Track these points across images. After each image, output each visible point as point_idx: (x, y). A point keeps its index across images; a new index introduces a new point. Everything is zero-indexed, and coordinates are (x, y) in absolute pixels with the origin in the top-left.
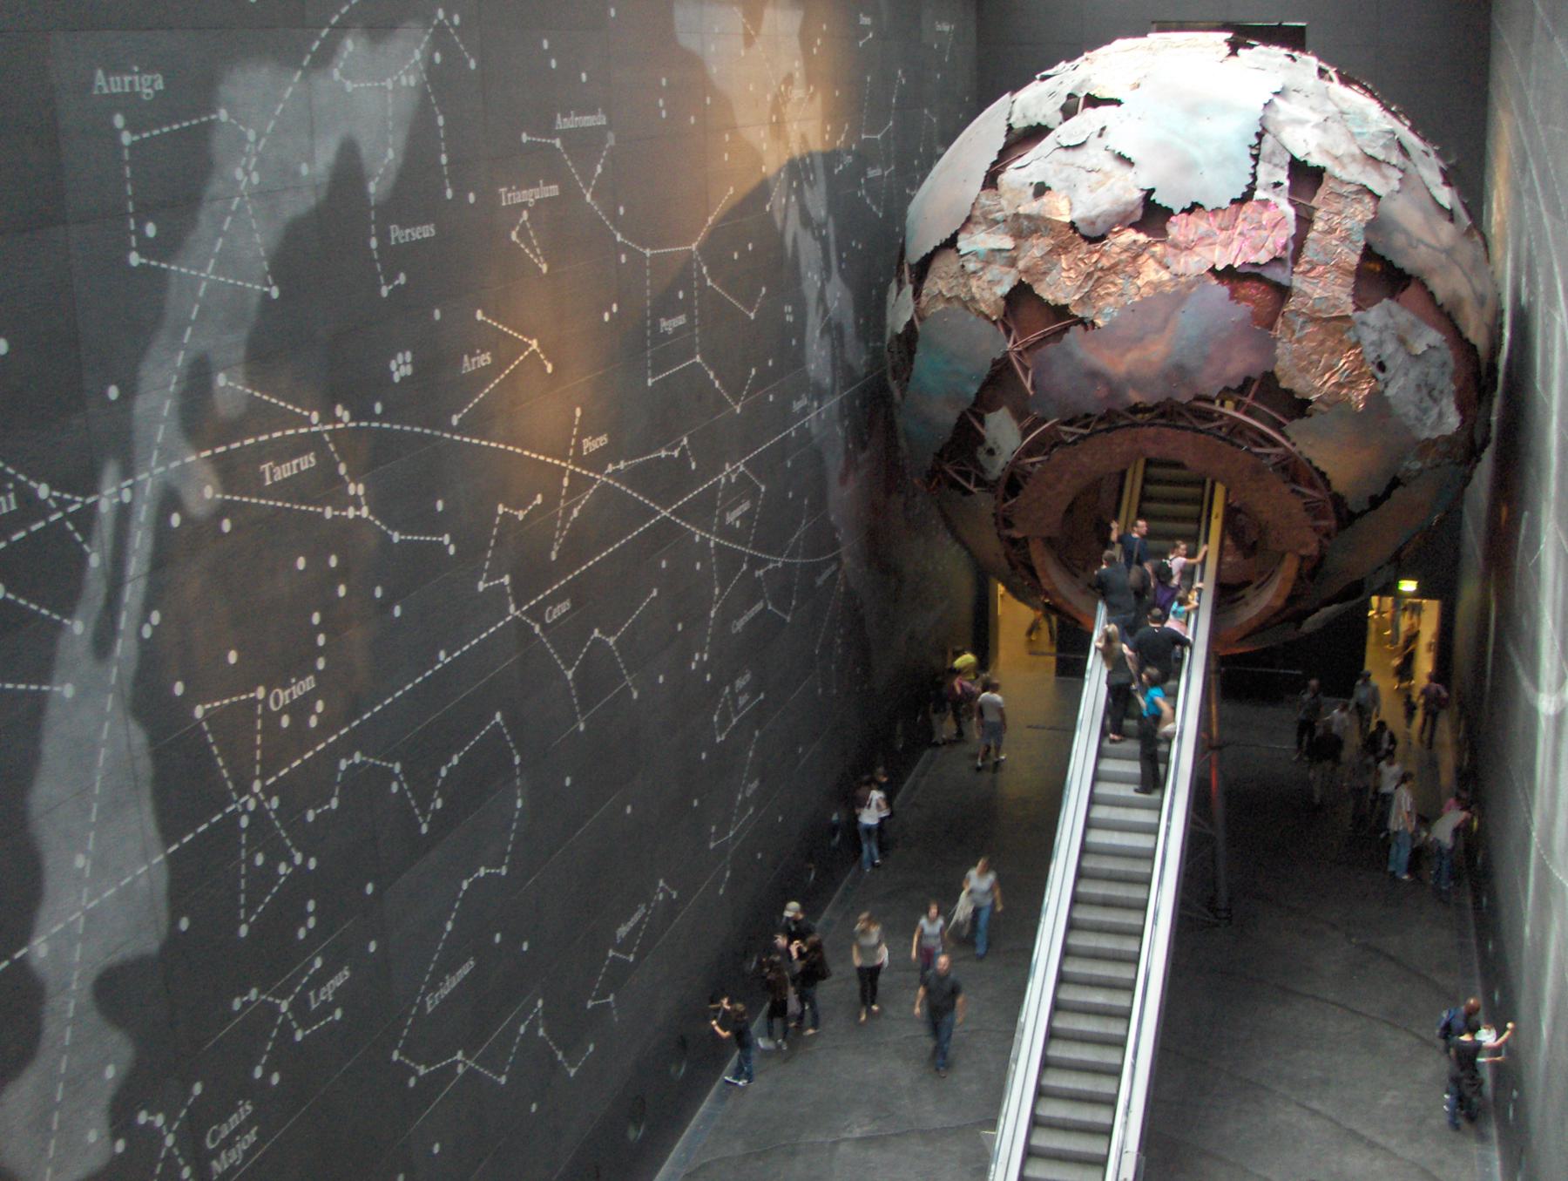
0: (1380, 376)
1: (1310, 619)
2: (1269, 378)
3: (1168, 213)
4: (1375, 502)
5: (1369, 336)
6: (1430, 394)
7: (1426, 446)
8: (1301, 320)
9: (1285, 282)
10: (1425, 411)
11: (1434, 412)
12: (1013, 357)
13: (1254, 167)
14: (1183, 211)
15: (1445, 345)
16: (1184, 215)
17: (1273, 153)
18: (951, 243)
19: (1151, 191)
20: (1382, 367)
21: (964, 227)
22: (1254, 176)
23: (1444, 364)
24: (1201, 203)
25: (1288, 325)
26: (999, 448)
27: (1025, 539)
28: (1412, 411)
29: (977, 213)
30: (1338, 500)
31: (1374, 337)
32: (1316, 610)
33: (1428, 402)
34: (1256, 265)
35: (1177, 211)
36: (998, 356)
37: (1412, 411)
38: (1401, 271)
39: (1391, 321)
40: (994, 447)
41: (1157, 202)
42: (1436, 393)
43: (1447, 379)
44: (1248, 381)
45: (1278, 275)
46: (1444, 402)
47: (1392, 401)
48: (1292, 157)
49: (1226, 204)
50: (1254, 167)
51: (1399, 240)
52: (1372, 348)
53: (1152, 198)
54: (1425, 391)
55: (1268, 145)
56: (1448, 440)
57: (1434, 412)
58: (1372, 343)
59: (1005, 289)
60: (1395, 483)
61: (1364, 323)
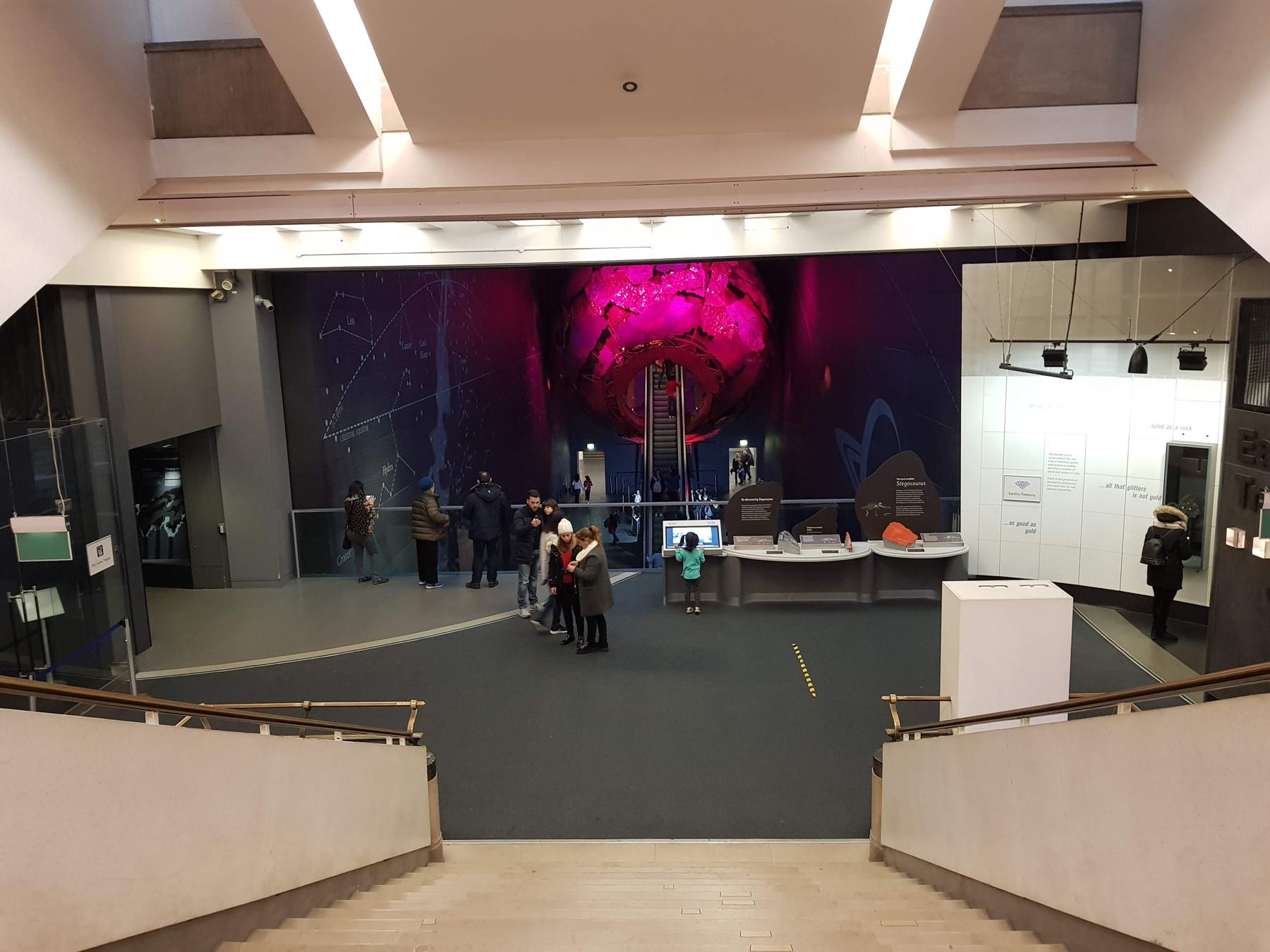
2: (700, 329)
4: (738, 373)
7: (753, 354)
9: (703, 296)
18: (583, 290)
21: (586, 285)
27: (615, 397)
29: (593, 280)
30: (724, 372)
32: (718, 419)
37: (748, 341)
38: (741, 292)
44: (693, 330)
51: (740, 281)
56: (761, 352)
59: (606, 304)
60: (743, 367)
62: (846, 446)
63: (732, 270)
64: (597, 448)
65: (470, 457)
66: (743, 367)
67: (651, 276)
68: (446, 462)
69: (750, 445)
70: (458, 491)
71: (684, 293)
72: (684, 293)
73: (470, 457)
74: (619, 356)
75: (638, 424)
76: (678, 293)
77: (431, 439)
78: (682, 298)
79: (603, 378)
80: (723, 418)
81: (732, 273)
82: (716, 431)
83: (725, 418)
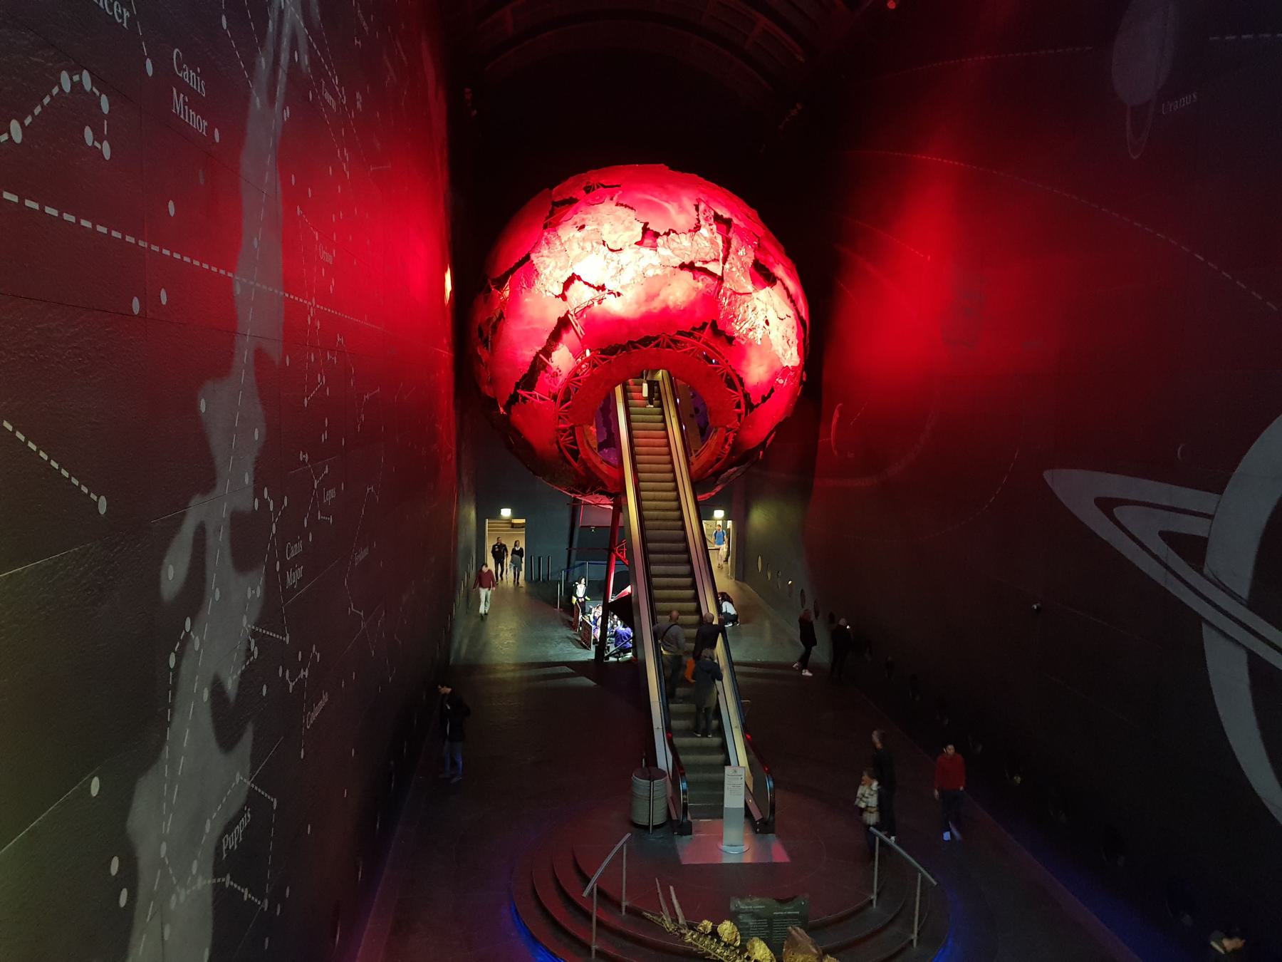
0: (766, 326)
1: (722, 476)
2: (714, 324)
3: (657, 235)
4: (764, 399)
5: (760, 306)
6: (788, 342)
8: (728, 293)
10: (785, 351)
11: (789, 353)
12: (569, 315)
13: (698, 215)
14: (665, 234)
15: (792, 317)
16: (665, 237)
17: (705, 211)
18: (528, 258)
19: (646, 224)
20: (767, 323)
22: (698, 220)
23: (793, 327)
24: (674, 229)
25: (725, 294)
26: (560, 371)
28: (780, 351)
30: (746, 396)
31: (764, 306)
33: (787, 347)
34: (706, 262)
35: (662, 234)
36: (562, 315)
39: (770, 299)
40: (558, 371)
41: (651, 229)
42: (790, 342)
43: (795, 337)
44: (705, 325)
45: (715, 268)
46: (793, 349)
47: (772, 342)
48: (716, 213)
49: (686, 231)
50: (698, 215)
52: (762, 312)
53: (648, 227)
54: (786, 341)
57: (789, 353)
58: (763, 310)
60: (772, 391)
61: (757, 299)
62: (1107, 505)
63: (759, 241)
64: (516, 515)
65: (332, 494)
66: (772, 391)
67: (639, 239)
68: (258, 493)
69: (727, 518)
70: (293, 578)
71: (688, 267)
72: (688, 267)
73: (332, 494)
74: (582, 363)
75: (606, 472)
76: (683, 266)
77: (203, 408)
78: (687, 275)
79: (555, 397)
80: (732, 470)
81: (759, 244)
82: (718, 489)
83: (735, 469)
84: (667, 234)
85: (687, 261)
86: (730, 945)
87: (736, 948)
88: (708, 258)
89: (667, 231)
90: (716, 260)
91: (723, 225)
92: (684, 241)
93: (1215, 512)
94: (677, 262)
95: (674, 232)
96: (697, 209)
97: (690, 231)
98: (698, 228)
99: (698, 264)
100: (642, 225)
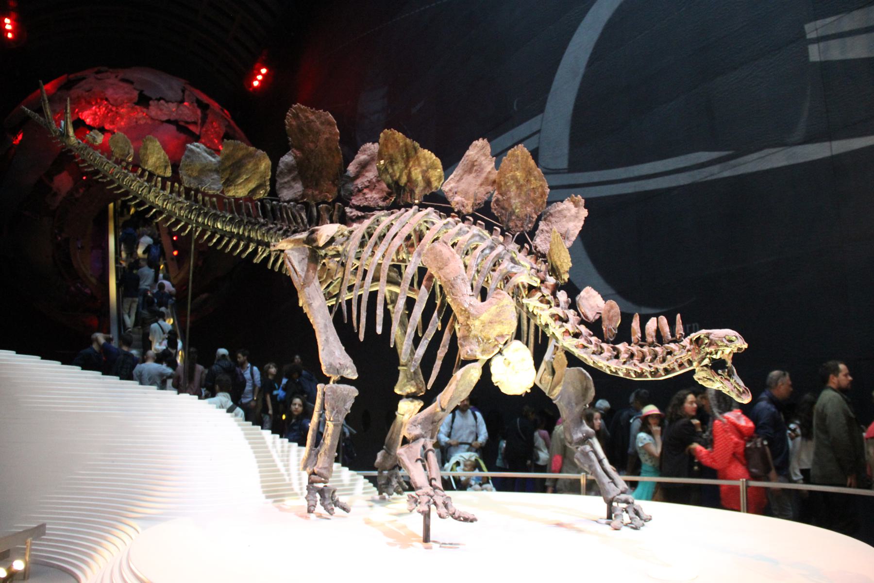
3: (150, 99)
9: (198, 133)
16: (156, 102)
55: (187, 93)
76: (169, 121)
78: (173, 128)
84: (159, 100)
85: (172, 118)
86: (122, 160)
87: (128, 164)
88: (189, 120)
89: (158, 97)
90: (195, 123)
91: (204, 107)
92: (173, 107)
93: (539, 143)
94: (165, 118)
95: (163, 99)
96: (183, 91)
97: (176, 101)
98: (182, 102)
99: (182, 124)
100: (138, 92)
